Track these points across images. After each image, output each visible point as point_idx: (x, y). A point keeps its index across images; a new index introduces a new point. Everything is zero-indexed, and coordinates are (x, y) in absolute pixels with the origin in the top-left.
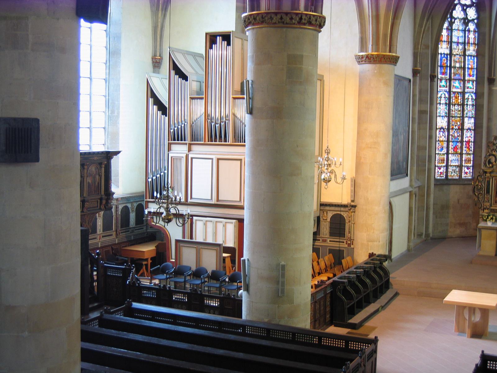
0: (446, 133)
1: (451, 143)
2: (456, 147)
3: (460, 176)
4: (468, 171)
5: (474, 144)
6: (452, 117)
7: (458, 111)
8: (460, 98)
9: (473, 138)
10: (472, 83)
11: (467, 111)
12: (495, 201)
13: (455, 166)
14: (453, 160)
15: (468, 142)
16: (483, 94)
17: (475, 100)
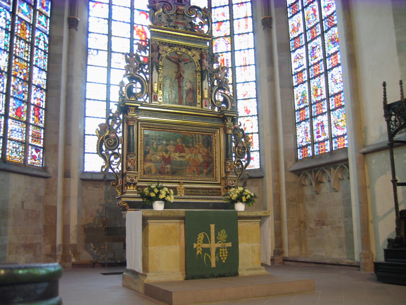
0: (5, 80)
1: (12, 101)
2: (19, 110)
3: (25, 160)
4: (37, 155)
5: (45, 113)
6: (16, 57)
7: (25, 51)
8: (28, 32)
9: (44, 103)
10: (45, 19)
11: (37, 57)
12: (144, 169)
13: (18, 141)
14: (15, 130)
15: (37, 107)
16: (61, 39)
17: (49, 45)
